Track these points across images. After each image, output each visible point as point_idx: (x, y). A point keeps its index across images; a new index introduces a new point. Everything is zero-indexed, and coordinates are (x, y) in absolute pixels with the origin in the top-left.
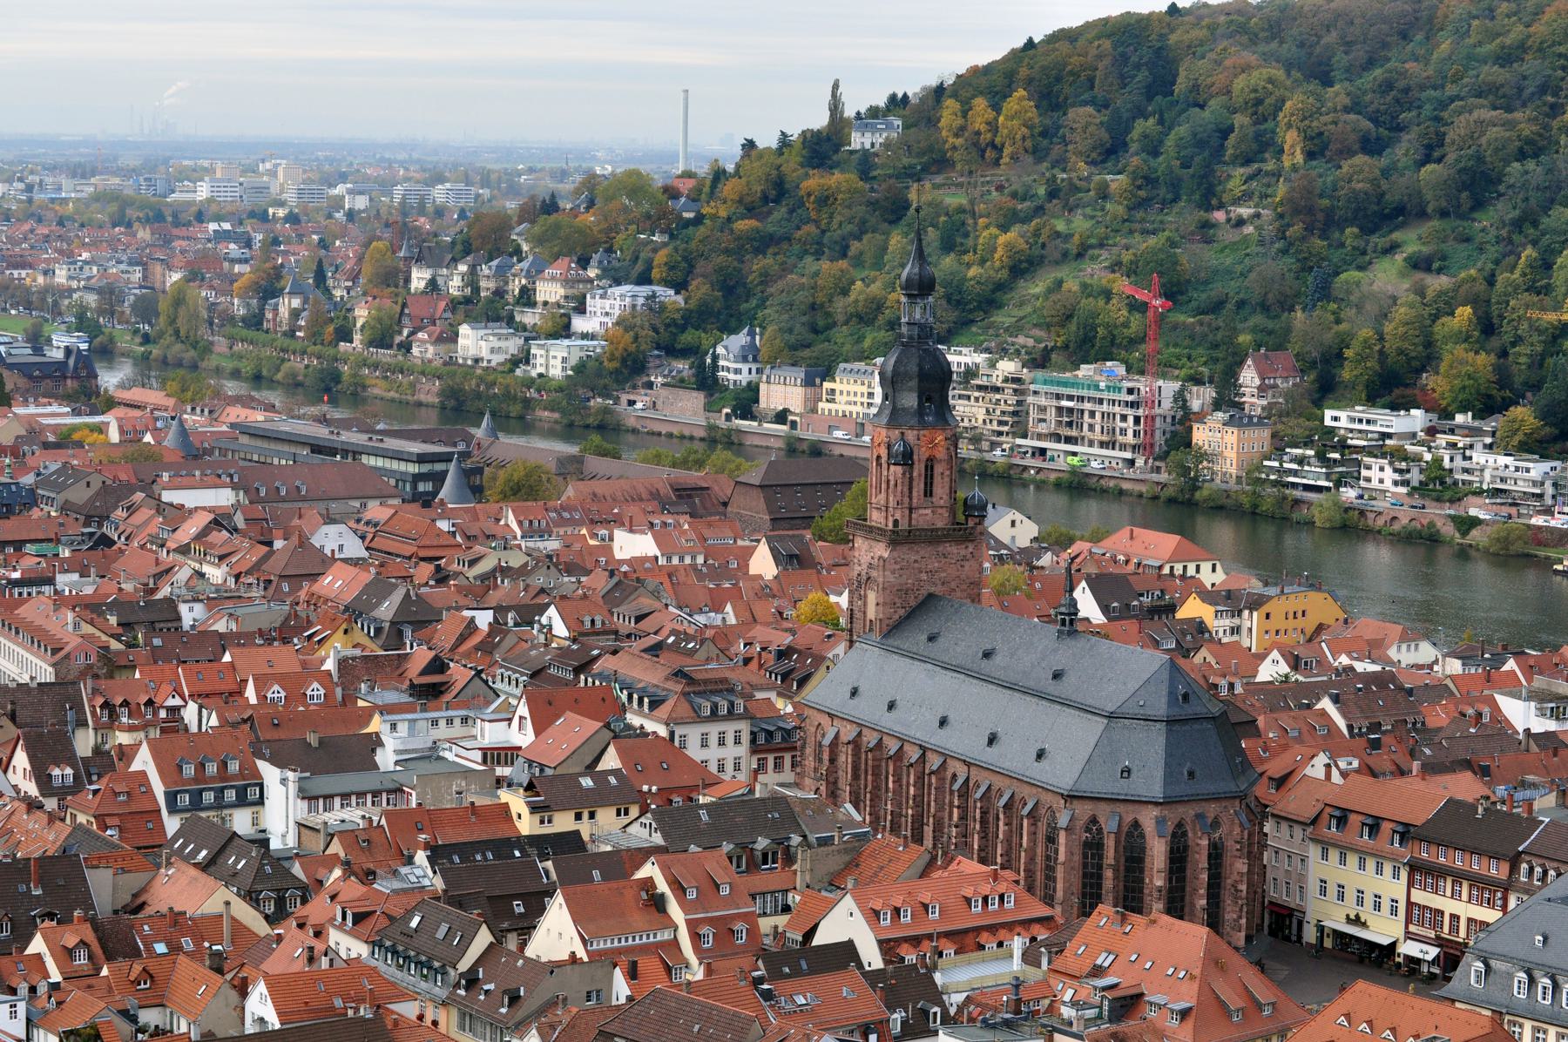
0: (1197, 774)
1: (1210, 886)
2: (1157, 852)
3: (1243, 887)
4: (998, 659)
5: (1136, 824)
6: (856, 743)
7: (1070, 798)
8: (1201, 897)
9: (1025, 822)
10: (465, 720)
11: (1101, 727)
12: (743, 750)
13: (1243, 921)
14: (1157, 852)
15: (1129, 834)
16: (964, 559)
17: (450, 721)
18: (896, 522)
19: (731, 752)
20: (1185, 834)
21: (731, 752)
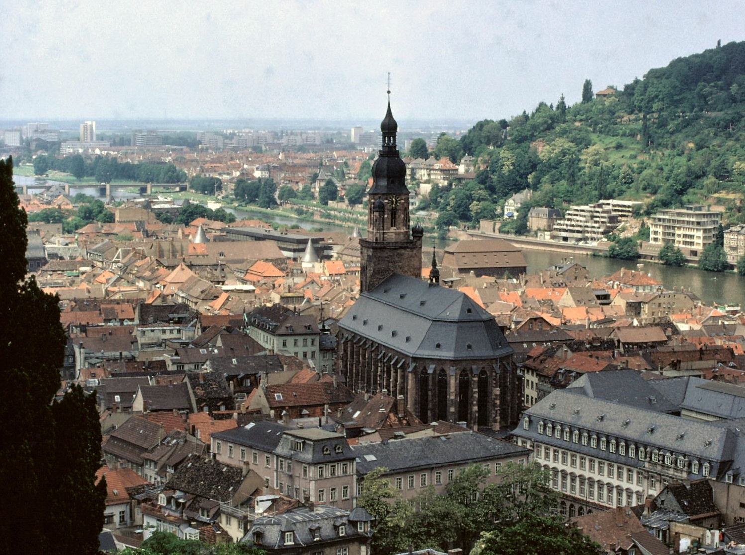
0: (473, 346)
1: (479, 401)
2: (453, 383)
3: (498, 402)
4: (405, 299)
5: (443, 370)
6: (351, 341)
7: (415, 359)
8: (475, 405)
9: (399, 370)
10: (179, 331)
11: (429, 325)
12: (316, 348)
13: (498, 418)
14: (453, 383)
15: (440, 375)
16: (411, 256)
17: (171, 331)
18: (376, 239)
19: (309, 349)
20: (467, 375)
21: (309, 349)
